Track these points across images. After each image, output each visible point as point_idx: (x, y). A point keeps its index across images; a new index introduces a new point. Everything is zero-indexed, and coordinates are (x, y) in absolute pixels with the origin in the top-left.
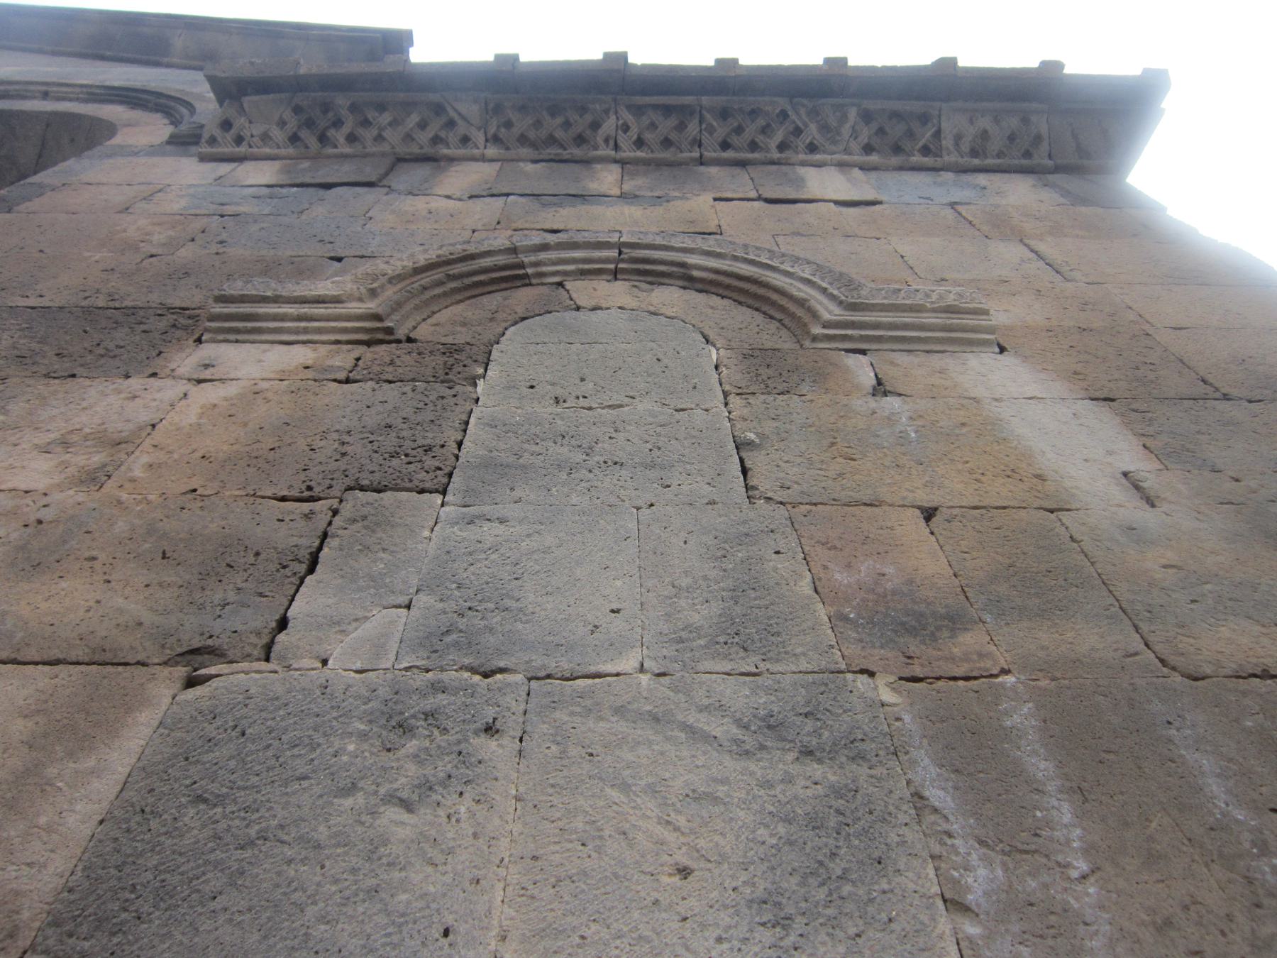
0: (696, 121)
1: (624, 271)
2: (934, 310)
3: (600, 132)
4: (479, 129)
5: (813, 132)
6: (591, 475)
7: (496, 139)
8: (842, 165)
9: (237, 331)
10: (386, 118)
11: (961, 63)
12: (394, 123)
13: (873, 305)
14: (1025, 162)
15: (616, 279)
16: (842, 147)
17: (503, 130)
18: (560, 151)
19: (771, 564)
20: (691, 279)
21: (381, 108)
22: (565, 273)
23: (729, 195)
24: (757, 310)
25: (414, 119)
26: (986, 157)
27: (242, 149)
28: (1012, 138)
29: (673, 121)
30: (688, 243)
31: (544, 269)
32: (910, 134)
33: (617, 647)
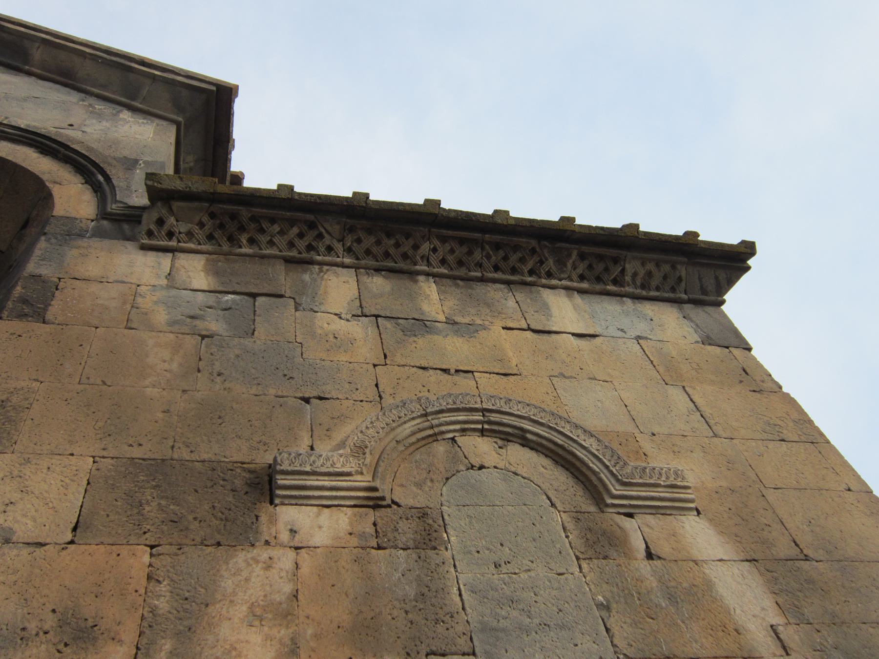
0: (479, 249)
1: (487, 430)
3: (419, 252)
4: (339, 241)
5: (550, 264)
7: (349, 250)
8: (566, 288)
9: (295, 497)
10: (276, 228)
11: (642, 229)
12: (282, 233)
14: (672, 295)
16: (566, 276)
17: (355, 244)
18: (393, 264)
20: (526, 439)
21: (273, 221)
22: (454, 431)
23: (511, 325)
25: (295, 230)
26: (650, 290)
27: (173, 243)
28: (665, 277)
29: (465, 249)
31: (444, 428)
32: (607, 269)
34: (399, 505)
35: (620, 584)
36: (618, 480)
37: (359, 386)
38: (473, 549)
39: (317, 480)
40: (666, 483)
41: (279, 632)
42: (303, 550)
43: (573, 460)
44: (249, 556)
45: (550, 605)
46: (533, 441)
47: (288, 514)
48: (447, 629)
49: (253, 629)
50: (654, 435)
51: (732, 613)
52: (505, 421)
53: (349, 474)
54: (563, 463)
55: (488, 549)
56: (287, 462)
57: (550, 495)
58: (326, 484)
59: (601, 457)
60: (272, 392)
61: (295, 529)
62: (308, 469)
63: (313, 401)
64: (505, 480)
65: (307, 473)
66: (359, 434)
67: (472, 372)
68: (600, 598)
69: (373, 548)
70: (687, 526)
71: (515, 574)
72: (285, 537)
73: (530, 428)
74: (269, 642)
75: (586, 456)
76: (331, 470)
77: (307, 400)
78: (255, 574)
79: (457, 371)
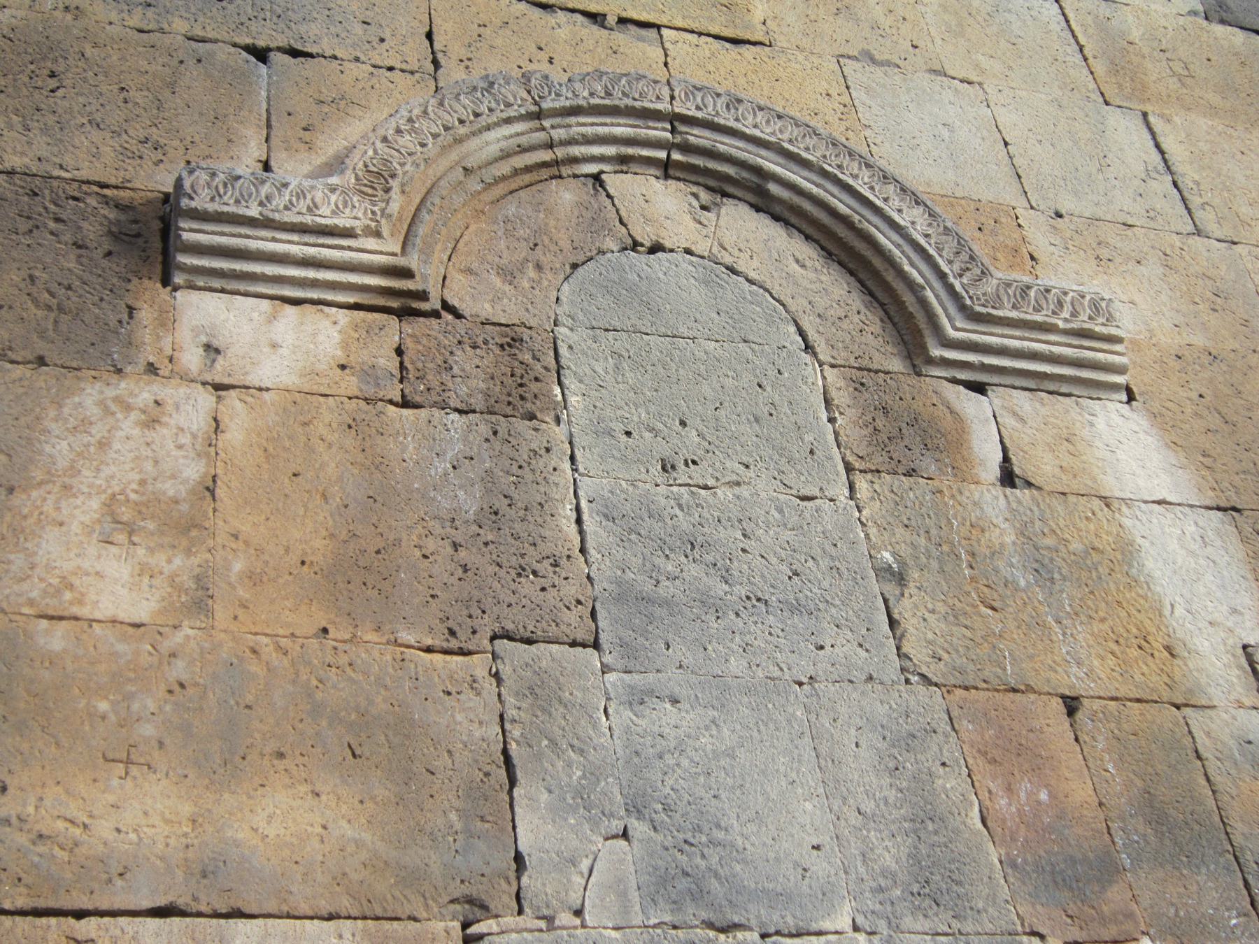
1: (679, 165)
2: (1066, 332)
6: (739, 622)
13: (1000, 318)
19: (940, 782)
20: (762, 192)
22: (602, 159)
30: (765, 132)
31: (577, 151)
33: (826, 897)
34: (458, 315)
35: (934, 532)
36: (963, 308)
37: (387, 36)
38: (619, 427)
39: (274, 240)
40: (1069, 326)
41: (169, 561)
42: (233, 393)
43: (868, 253)
44: (110, 393)
45: (774, 561)
46: (780, 201)
47: (202, 310)
48: (543, 589)
49: (114, 550)
50: (1060, 216)
51: (1167, 612)
52: (722, 148)
53: (348, 233)
54: (843, 257)
55: (651, 430)
56: (205, 193)
57: (806, 325)
58: (295, 250)
59: (932, 251)
60: (180, 26)
61: (216, 343)
62: (254, 211)
63: (276, 57)
64: (707, 283)
65: (251, 222)
66: (379, 145)
67: (658, 27)
68: (887, 556)
69: (391, 402)
70: (1100, 423)
71: (706, 488)
72: (192, 358)
73: (778, 170)
74: (146, 580)
75: (898, 246)
76: (308, 219)
77: (261, 55)
78: (120, 433)
79: (622, 21)
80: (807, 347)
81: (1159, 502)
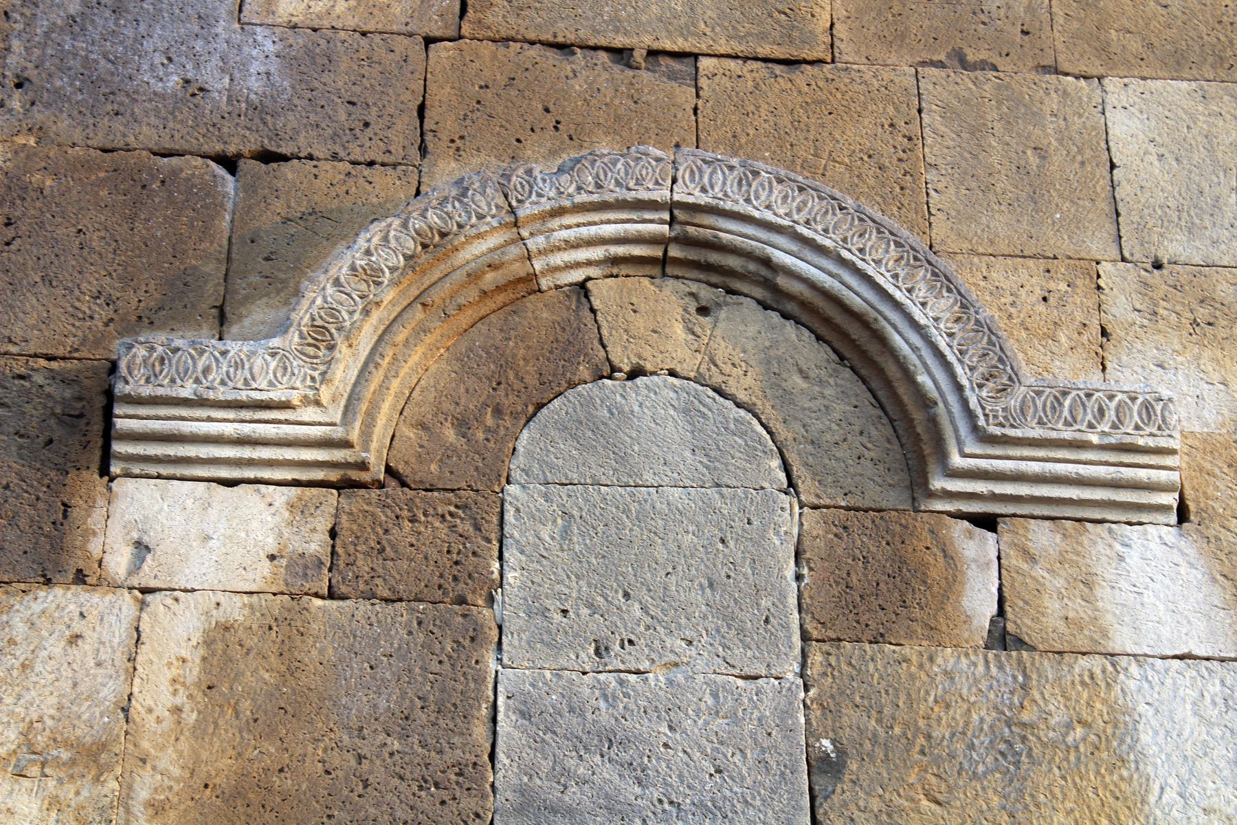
1: (677, 262)
15: (664, 275)
22: (589, 263)
24: (864, 381)
35: (887, 711)
36: (975, 428)
37: (371, 118)
38: (553, 605)
39: (210, 419)
40: (1107, 441)
41: (78, 793)
42: (158, 595)
44: (37, 607)
45: (697, 755)
46: (790, 297)
48: (443, 803)
49: (26, 783)
50: (1158, 266)
51: (1152, 799)
53: (285, 406)
54: (857, 363)
55: (590, 605)
56: (140, 373)
57: (792, 458)
59: (951, 358)
61: (146, 539)
62: (187, 392)
63: (246, 165)
64: (686, 411)
65: (186, 403)
66: (330, 290)
67: (696, 56)
68: (826, 743)
69: (316, 595)
70: (1133, 558)
71: (638, 672)
72: (119, 562)
73: (788, 260)
74: (54, 814)
75: (915, 349)
76: (243, 396)
78: (44, 654)
79: (653, 53)
80: (791, 484)
81: (1181, 657)
